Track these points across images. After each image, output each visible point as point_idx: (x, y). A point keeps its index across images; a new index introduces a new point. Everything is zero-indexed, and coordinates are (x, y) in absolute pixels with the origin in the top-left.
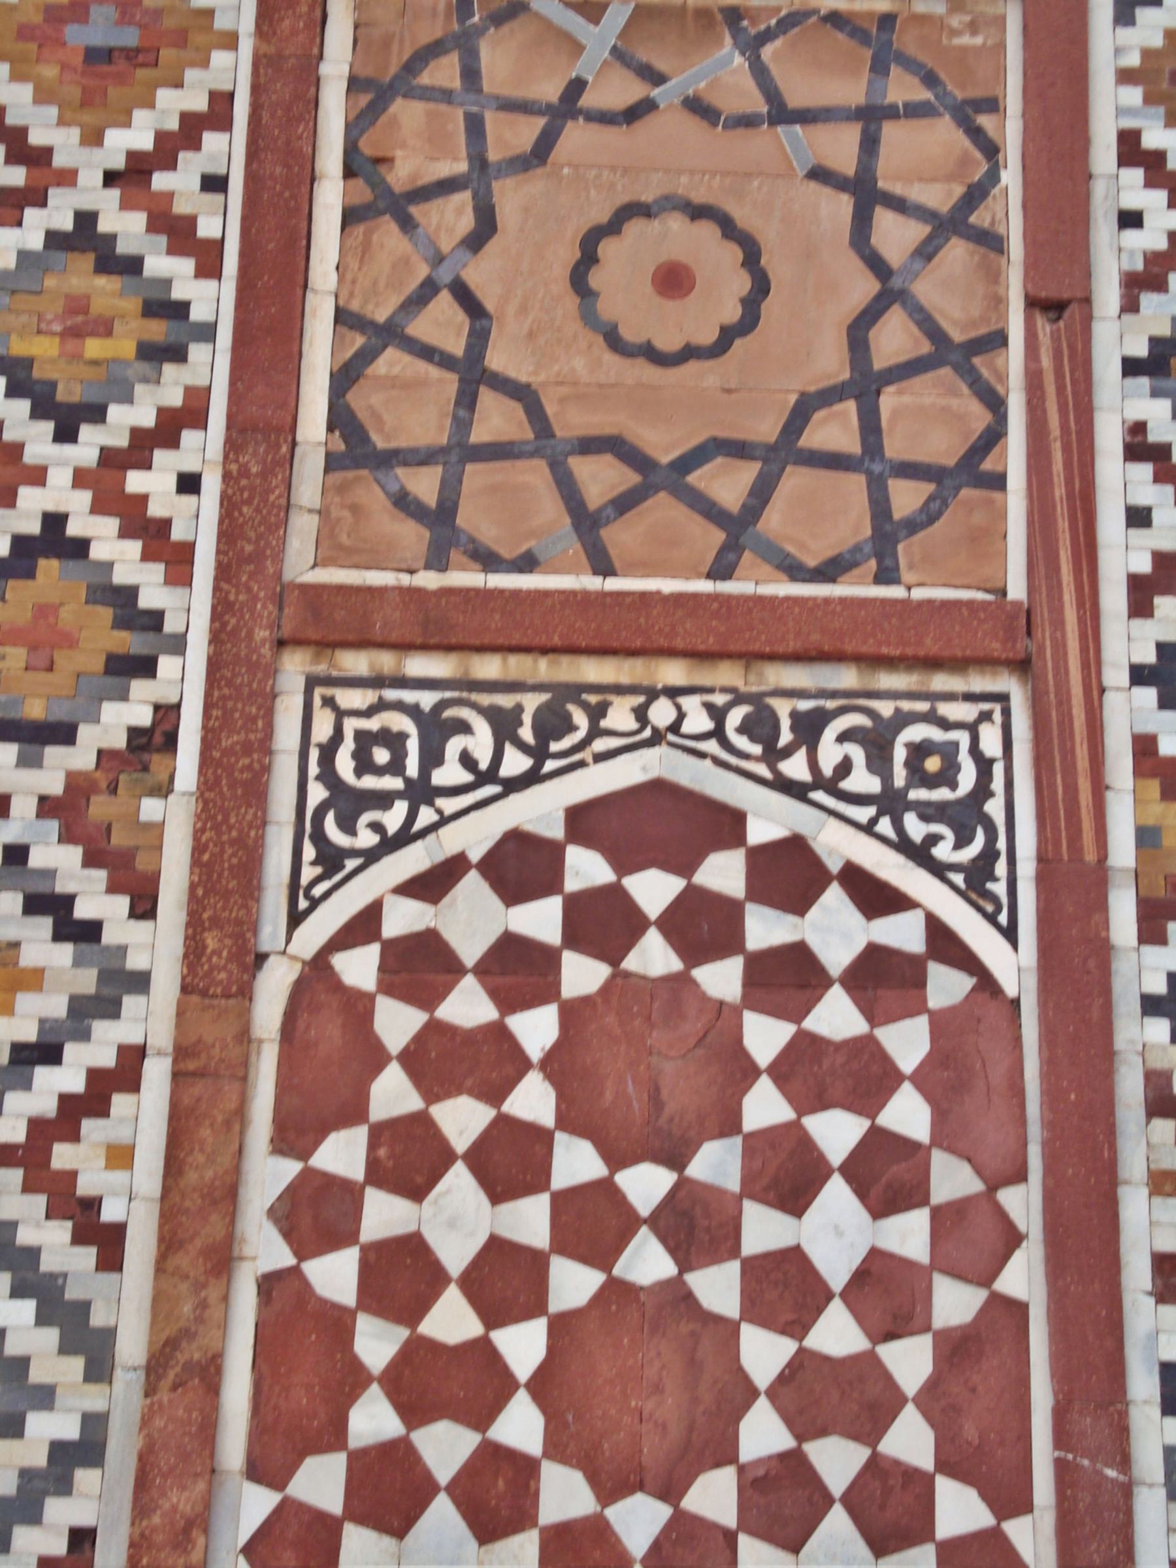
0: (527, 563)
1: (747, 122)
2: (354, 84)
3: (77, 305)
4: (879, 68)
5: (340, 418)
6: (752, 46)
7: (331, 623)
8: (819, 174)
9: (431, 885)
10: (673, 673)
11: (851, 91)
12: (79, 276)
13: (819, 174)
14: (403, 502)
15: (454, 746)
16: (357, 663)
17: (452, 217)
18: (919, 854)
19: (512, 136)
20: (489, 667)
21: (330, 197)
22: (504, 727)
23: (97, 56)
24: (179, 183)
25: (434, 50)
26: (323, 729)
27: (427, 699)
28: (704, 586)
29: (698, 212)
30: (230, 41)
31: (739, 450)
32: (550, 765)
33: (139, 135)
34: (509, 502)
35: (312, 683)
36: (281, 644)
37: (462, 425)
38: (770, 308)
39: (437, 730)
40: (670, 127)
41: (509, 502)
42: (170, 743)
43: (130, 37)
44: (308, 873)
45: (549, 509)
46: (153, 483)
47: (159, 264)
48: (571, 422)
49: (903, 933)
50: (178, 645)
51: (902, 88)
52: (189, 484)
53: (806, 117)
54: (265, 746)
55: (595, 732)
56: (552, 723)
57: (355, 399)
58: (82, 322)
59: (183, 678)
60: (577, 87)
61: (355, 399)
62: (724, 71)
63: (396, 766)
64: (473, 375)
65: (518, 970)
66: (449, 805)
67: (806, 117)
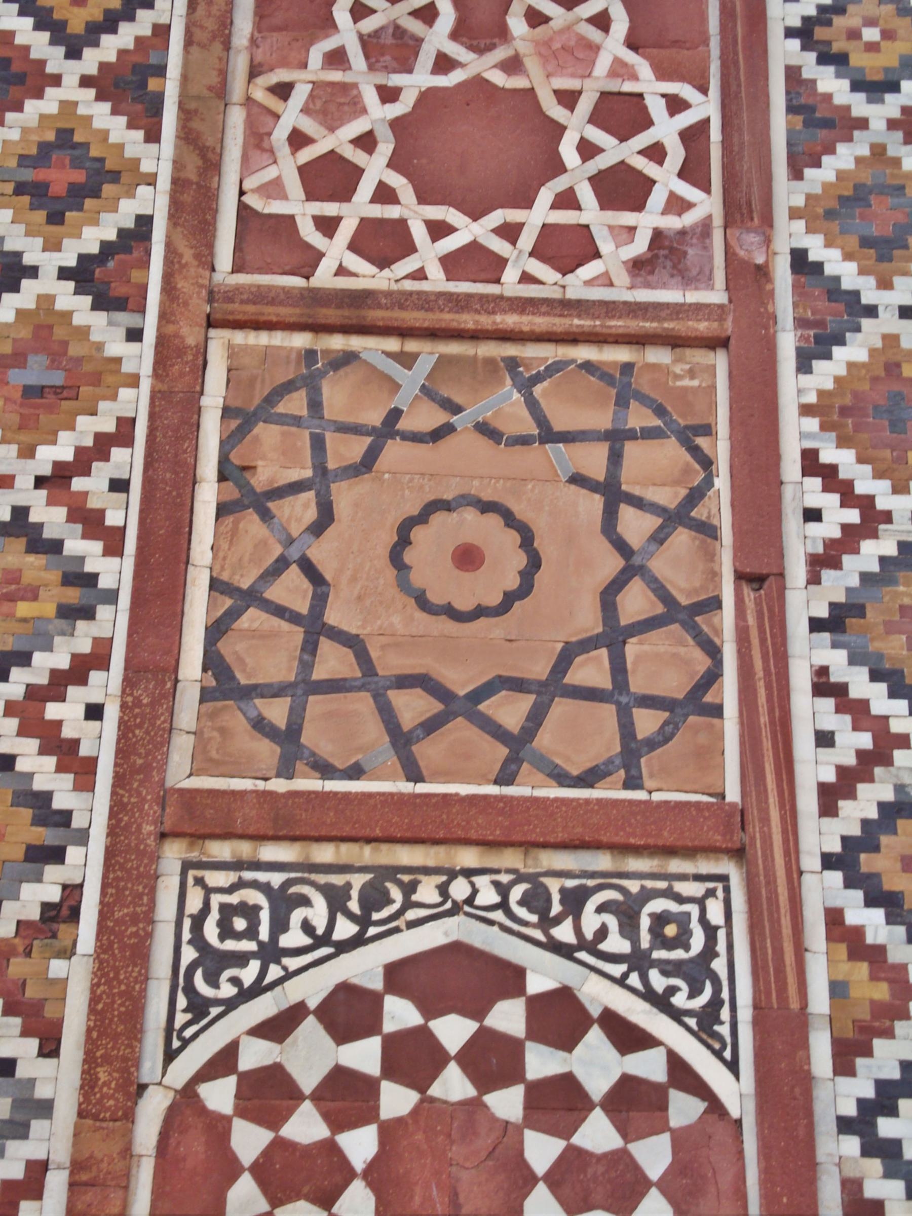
0: (355, 772)
1: (524, 441)
2: (227, 412)
4: (622, 402)
5: (212, 661)
6: (526, 386)
7: (203, 818)
8: (577, 479)
9: (277, 1028)
10: (468, 857)
11: (601, 419)
13: (577, 479)
14: (260, 725)
15: (297, 916)
16: (222, 850)
17: (300, 511)
18: (661, 1002)
19: (346, 450)
20: (325, 853)
21: (207, 496)
22: (336, 900)
23: (32, 392)
24: (92, 485)
25: (288, 387)
26: (194, 904)
27: (276, 879)
28: (493, 790)
29: (486, 507)
30: (134, 381)
31: (518, 685)
32: (372, 931)
33: (63, 450)
34: (342, 726)
35: (187, 866)
36: (163, 836)
37: (306, 666)
38: (541, 578)
39: (284, 903)
40: (466, 446)
41: (342, 726)
42: (74, 915)
43: (57, 378)
44: (181, 1018)
45: (373, 731)
46: (67, 713)
47: (75, 545)
48: (390, 663)
49: (649, 1066)
50: (82, 838)
51: (639, 417)
52: (94, 712)
53: (567, 438)
54: (149, 917)
55: (408, 904)
56: (374, 898)
57: (225, 647)
59: (86, 863)
60: (395, 414)
61: (225, 647)
62: (506, 405)
63: (251, 933)
64: (315, 628)
65: (346, 1097)
66: (293, 963)
67: (567, 438)
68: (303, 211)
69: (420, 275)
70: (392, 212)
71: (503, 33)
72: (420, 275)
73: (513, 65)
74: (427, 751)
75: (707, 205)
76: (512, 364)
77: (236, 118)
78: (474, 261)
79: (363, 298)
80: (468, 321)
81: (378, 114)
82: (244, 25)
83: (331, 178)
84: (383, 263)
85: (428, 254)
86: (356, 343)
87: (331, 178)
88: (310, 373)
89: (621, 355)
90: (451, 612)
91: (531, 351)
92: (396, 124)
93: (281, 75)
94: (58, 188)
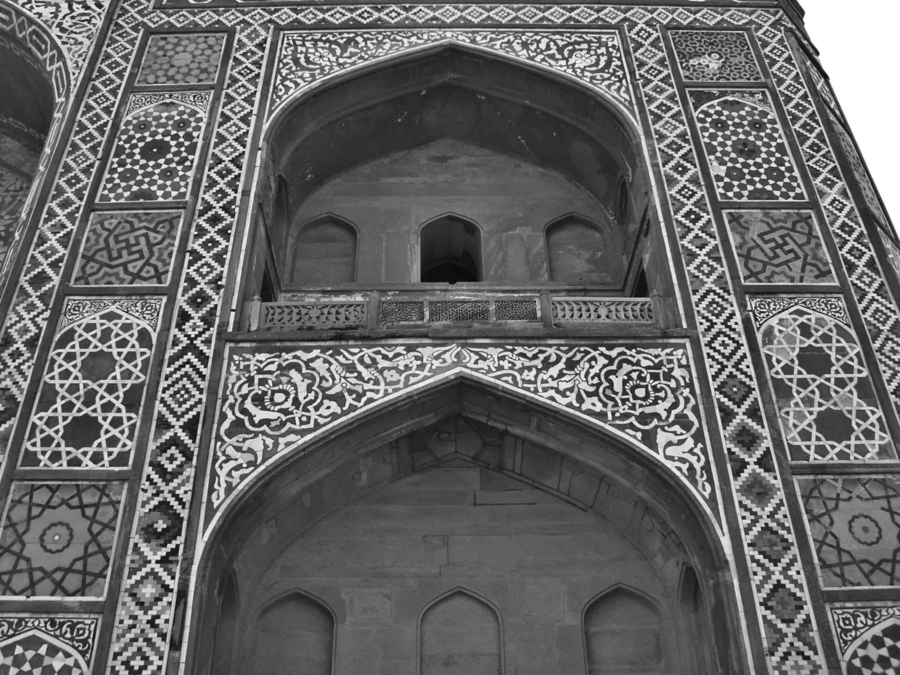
0: (859, 584)
1: (868, 499)
2: (803, 497)
3: (770, 541)
5: (820, 559)
6: (864, 485)
7: (832, 597)
8: (883, 509)
9: (864, 646)
10: (890, 604)
11: (883, 493)
12: (768, 536)
14: (836, 574)
16: (838, 605)
20: (859, 604)
21: (805, 518)
23: (759, 494)
24: (779, 516)
25: (812, 490)
29: (866, 517)
30: (779, 490)
33: (769, 509)
34: (853, 573)
37: (840, 559)
39: (855, 617)
40: (856, 501)
41: (853, 573)
43: (762, 490)
45: (859, 574)
47: (781, 532)
48: (858, 557)
50: (806, 603)
51: (891, 493)
52: (798, 573)
56: (874, 615)
57: (822, 555)
58: (772, 544)
59: (809, 608)
60: (838, 495)
61: (822, 555)
62: (860, 490)
68: (802, 444)
69: (832, 459)
70: (821, 443)
71: (831, 397)
72: (832, 459)
73: (835, 404)
74: (873, 578)
75: (888, 438)
76: (859, 480)
77: (780, 420)
78: (842, 455)
79: (823, 466)
80: (848, 470)
81: (811, 418)
82: (774, 398)
83: (805, 435)
84: (824, 456)
85: (832, 453)
86: (824, 477)
87: (805, 435)
88: (817, 485)
89: (881, 477)
90: (865, 543)
91: (862, 477)
92: (815, 420)
93: (786, 409)
94: (747, 441)
